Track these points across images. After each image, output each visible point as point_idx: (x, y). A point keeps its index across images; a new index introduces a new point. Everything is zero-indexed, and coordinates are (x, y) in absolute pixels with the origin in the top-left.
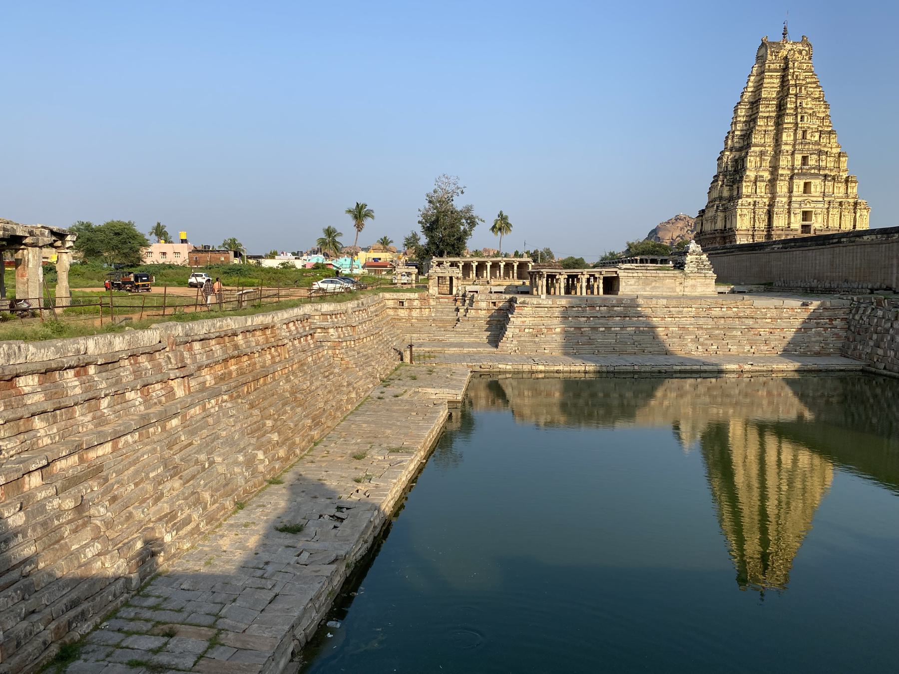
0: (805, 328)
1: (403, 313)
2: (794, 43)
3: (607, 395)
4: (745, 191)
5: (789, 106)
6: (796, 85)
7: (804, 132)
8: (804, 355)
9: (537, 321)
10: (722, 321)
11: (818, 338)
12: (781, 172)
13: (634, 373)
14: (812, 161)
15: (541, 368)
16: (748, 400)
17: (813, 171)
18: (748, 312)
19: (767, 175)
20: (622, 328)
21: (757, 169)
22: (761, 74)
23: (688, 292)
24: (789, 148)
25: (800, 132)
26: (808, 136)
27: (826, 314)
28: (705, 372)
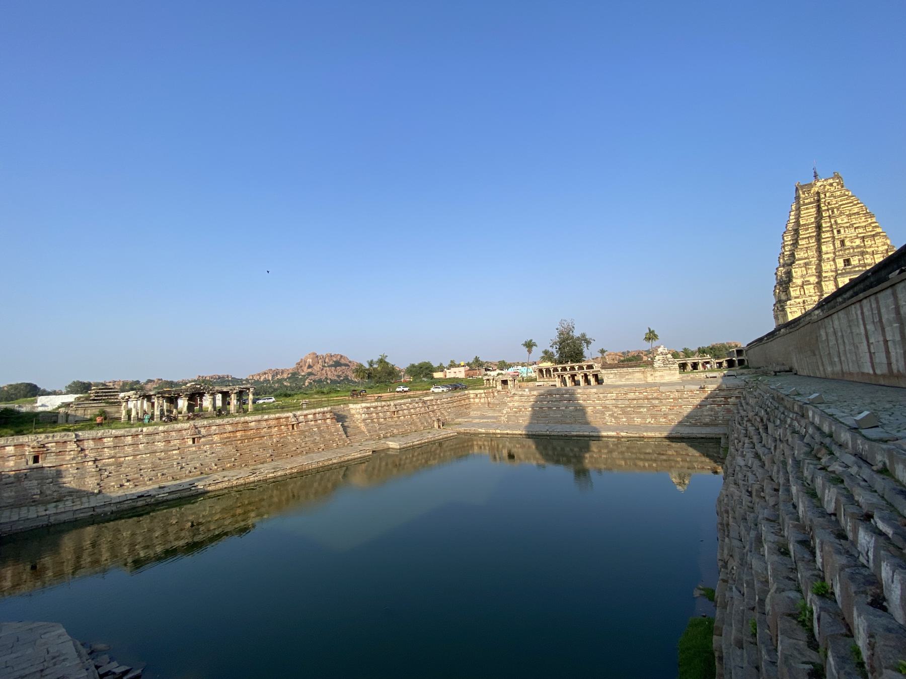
0: (701, 405)
1: (477, 400)
2: (826, 180)
3: (563, 449)
4: (793, 294)
5: (824, 225)
6: (828, 210)
7: (843, 243)
8: (695, 425)
9: (521, 404)
10: (635, 402)
11: (710, 413)
12: (824, 275)
13: (548, 436)
14: (855, 261)
15: (498, 431)
16: (664, 457)
17: (857, 269)
18: (655, 395)
19: (813, 279)
20: (566, 407)
21: (802, 276)
22: (798, 209)
23: (658, 380)
24: (831, 256)
25: (838, 244)
26: (848, 243)
27: (722, 393)
28: (593, 436)
